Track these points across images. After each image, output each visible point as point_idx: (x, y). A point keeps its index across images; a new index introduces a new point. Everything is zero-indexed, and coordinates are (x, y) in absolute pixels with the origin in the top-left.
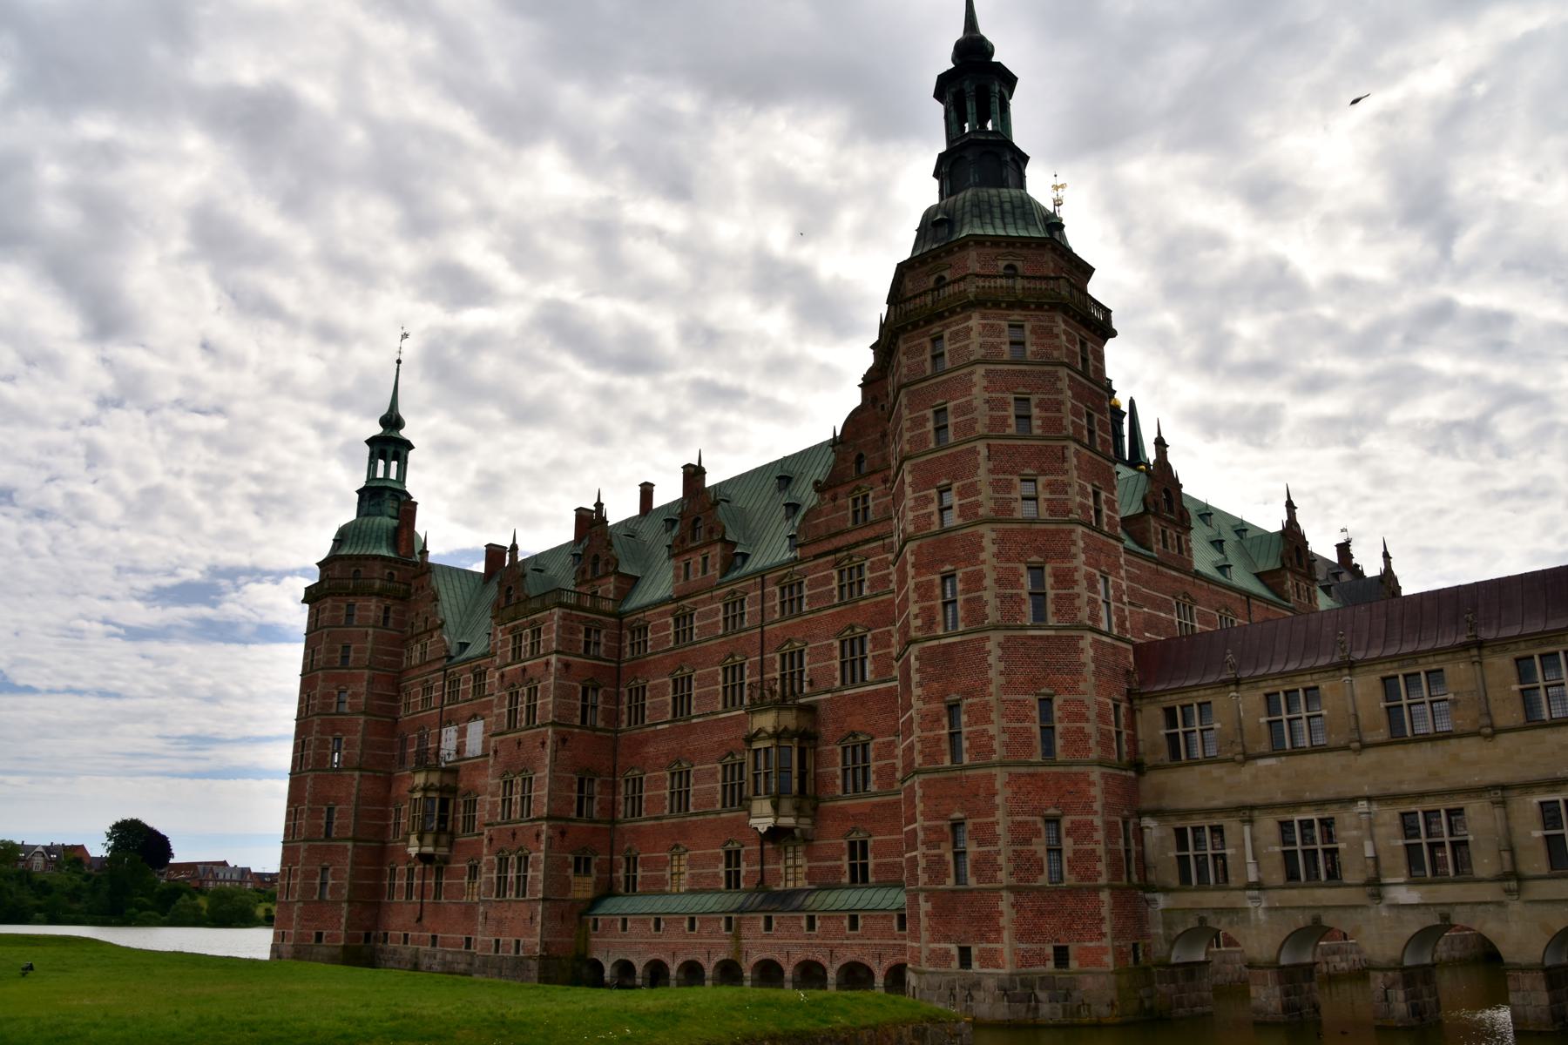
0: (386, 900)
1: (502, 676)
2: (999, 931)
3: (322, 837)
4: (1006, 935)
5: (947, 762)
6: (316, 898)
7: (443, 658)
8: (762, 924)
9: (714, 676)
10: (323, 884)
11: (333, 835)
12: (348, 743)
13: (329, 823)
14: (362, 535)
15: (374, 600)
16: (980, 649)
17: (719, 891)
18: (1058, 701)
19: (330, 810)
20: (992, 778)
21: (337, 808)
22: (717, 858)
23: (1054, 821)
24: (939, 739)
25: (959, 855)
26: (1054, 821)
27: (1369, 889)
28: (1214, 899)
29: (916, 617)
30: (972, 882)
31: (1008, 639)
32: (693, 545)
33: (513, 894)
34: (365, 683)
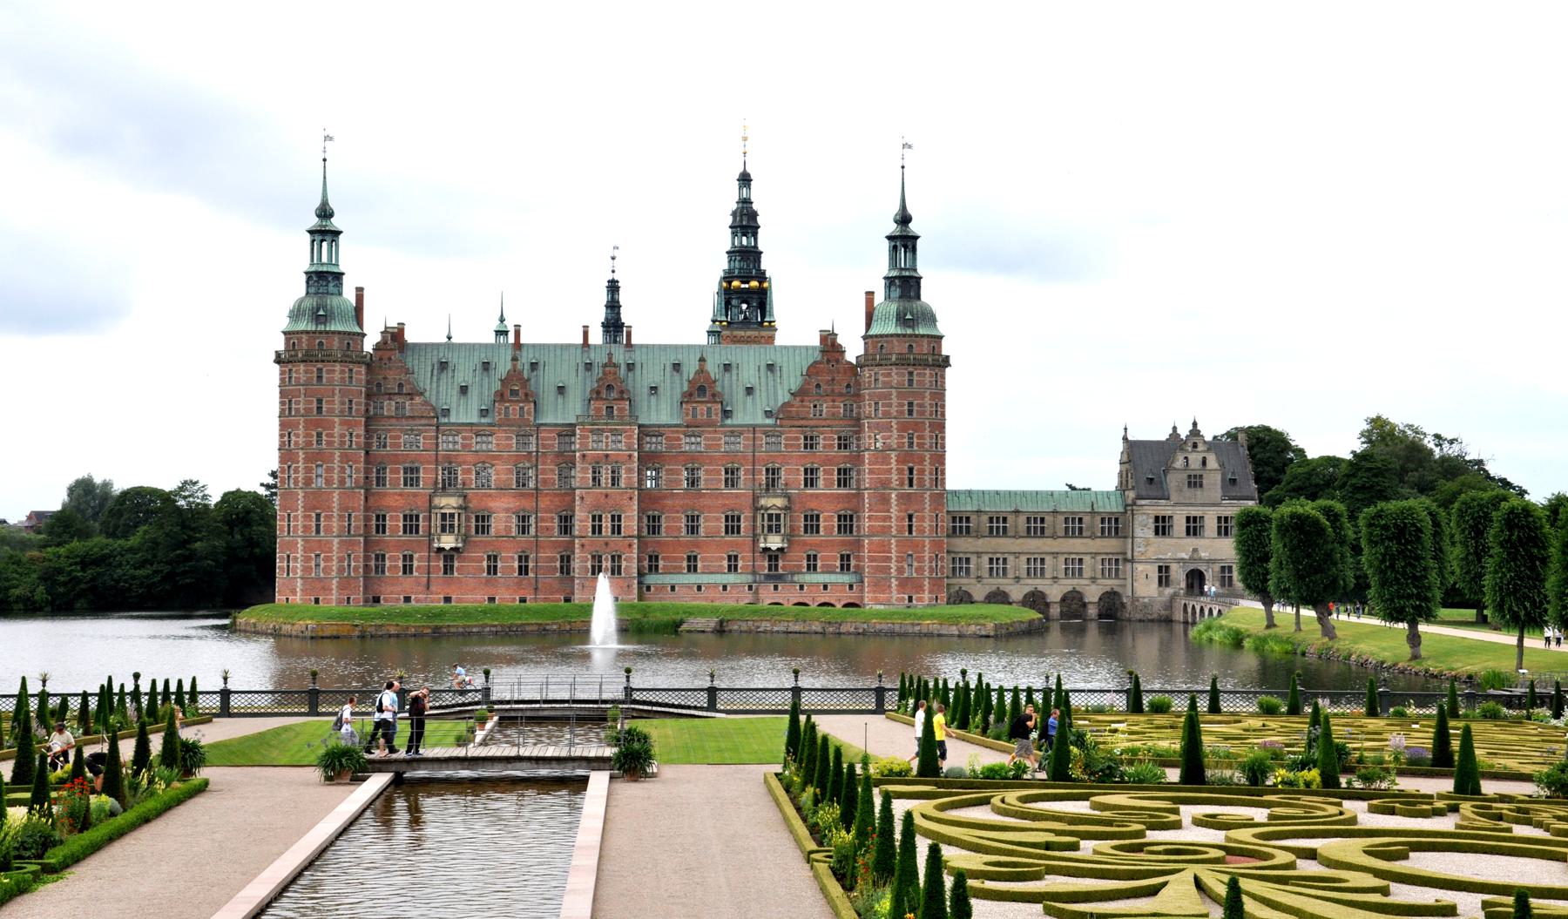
0: (373, 574)
1: (584, 456)
2: (924, 591)
4: (926, 592)
5: (907, 534)
6: (346, 574)
8: (772, 588)
9: (718, 472)
10: (349, 566)
11: (352, 532)
13: (349, 525)
16: (922, 496)
19: (350, 515)
20: (924, 542)
21: (353, 515)
22: (723, 559)
23: (937, 556)
24: (904, 526)
26: (937, 556)
28: (964, 581)
30: (915, 575)
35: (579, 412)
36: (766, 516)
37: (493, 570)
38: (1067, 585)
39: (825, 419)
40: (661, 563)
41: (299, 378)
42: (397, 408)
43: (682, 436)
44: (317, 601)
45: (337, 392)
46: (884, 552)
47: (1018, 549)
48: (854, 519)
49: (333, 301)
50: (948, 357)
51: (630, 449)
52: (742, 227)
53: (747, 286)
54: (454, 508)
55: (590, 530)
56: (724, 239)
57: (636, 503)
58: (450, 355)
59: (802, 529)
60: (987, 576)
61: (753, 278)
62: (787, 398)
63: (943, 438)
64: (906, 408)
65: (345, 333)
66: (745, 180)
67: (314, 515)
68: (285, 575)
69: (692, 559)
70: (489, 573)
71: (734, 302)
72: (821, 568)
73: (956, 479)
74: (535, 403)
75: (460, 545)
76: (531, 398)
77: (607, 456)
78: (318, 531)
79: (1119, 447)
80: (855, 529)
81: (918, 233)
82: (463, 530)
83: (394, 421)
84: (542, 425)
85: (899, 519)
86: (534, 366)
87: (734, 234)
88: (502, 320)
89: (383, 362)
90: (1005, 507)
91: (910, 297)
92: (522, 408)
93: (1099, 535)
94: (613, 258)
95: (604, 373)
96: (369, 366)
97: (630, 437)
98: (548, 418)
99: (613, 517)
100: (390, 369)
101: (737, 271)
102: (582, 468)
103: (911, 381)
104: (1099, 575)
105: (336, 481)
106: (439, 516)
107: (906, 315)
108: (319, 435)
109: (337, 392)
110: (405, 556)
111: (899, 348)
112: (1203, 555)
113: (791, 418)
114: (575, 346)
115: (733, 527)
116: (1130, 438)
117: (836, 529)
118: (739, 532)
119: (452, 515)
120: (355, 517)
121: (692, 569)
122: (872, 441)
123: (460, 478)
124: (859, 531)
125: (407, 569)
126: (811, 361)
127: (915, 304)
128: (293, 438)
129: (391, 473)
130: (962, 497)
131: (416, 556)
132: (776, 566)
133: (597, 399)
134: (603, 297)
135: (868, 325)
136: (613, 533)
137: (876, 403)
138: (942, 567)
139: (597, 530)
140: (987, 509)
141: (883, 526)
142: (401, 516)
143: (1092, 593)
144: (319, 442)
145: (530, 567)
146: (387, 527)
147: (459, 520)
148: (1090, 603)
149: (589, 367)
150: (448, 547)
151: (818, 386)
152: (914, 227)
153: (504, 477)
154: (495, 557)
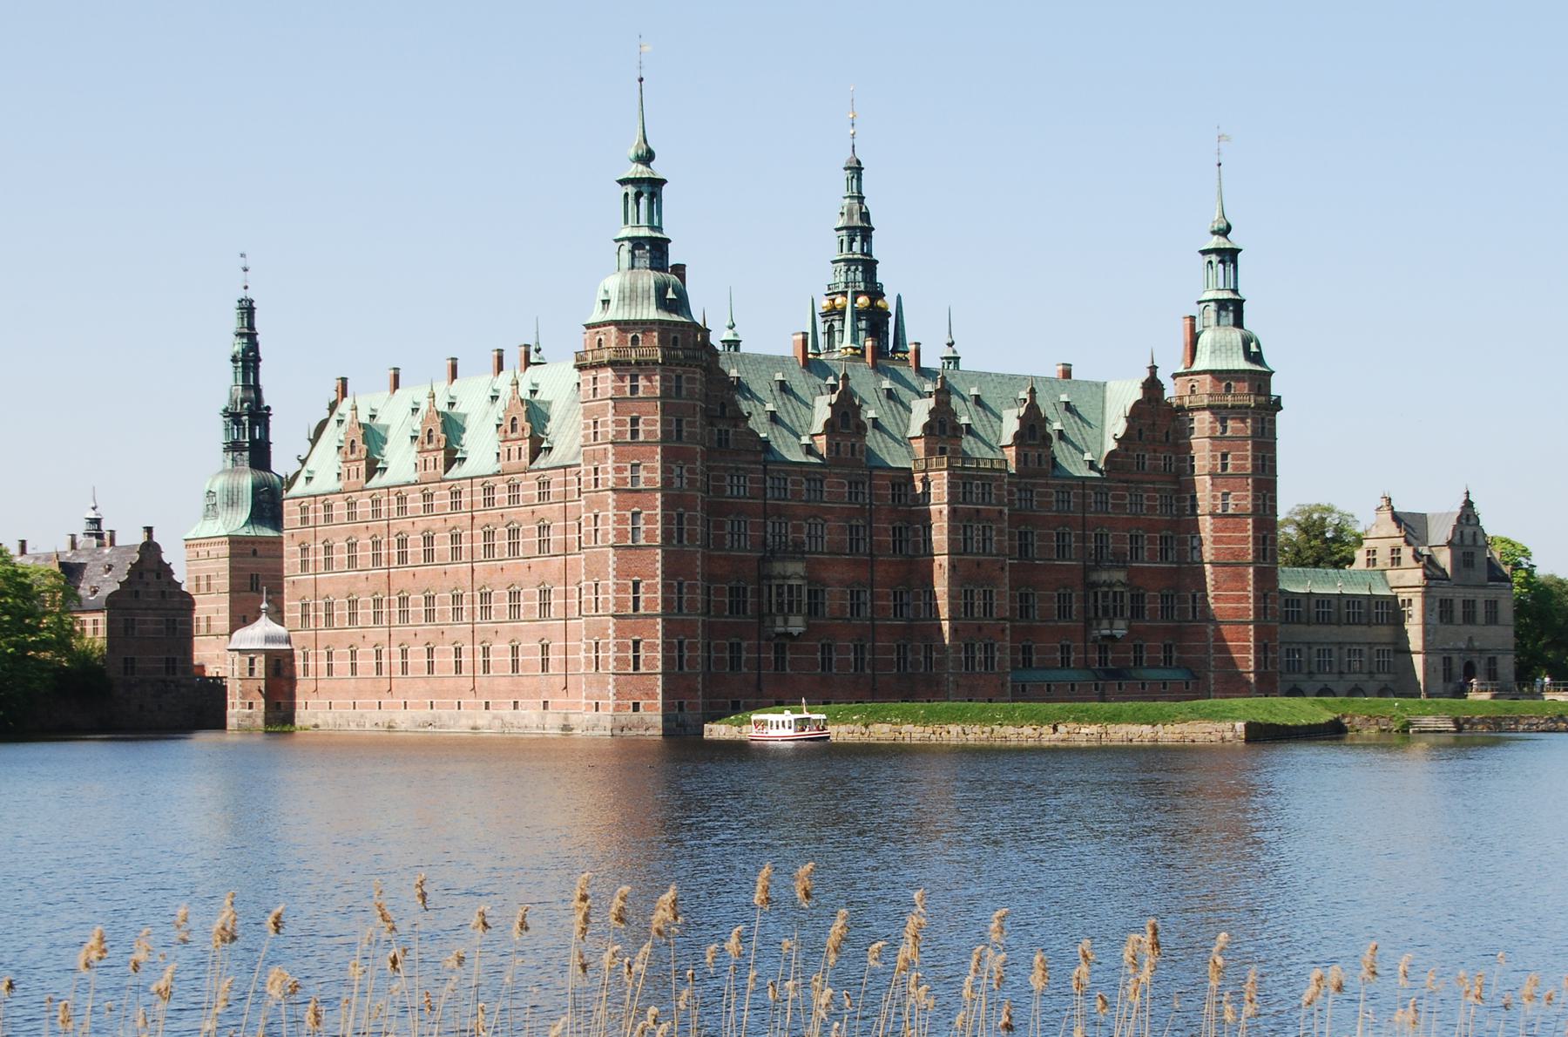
17: (1058, 668)
25: (1266, 658)
32: (1032, 442)
33: (983, 670)
37: (826, 664)
46: (1238, 640)
51: (1000, 503)
56: (831, 246)
57: (1007, 574)
70: (823, 669)
77: (978, 511)
78: (680, 609)
94: (246, 270)
97: (1000, 487)
105: (699, 537)
109: (698, 409)
112: (1476, 644)
128: (643, 474)
131: (744, 644)
134: (233, 322)
141: (1237, 609)
145: (867, 660)
150: (795, 634)
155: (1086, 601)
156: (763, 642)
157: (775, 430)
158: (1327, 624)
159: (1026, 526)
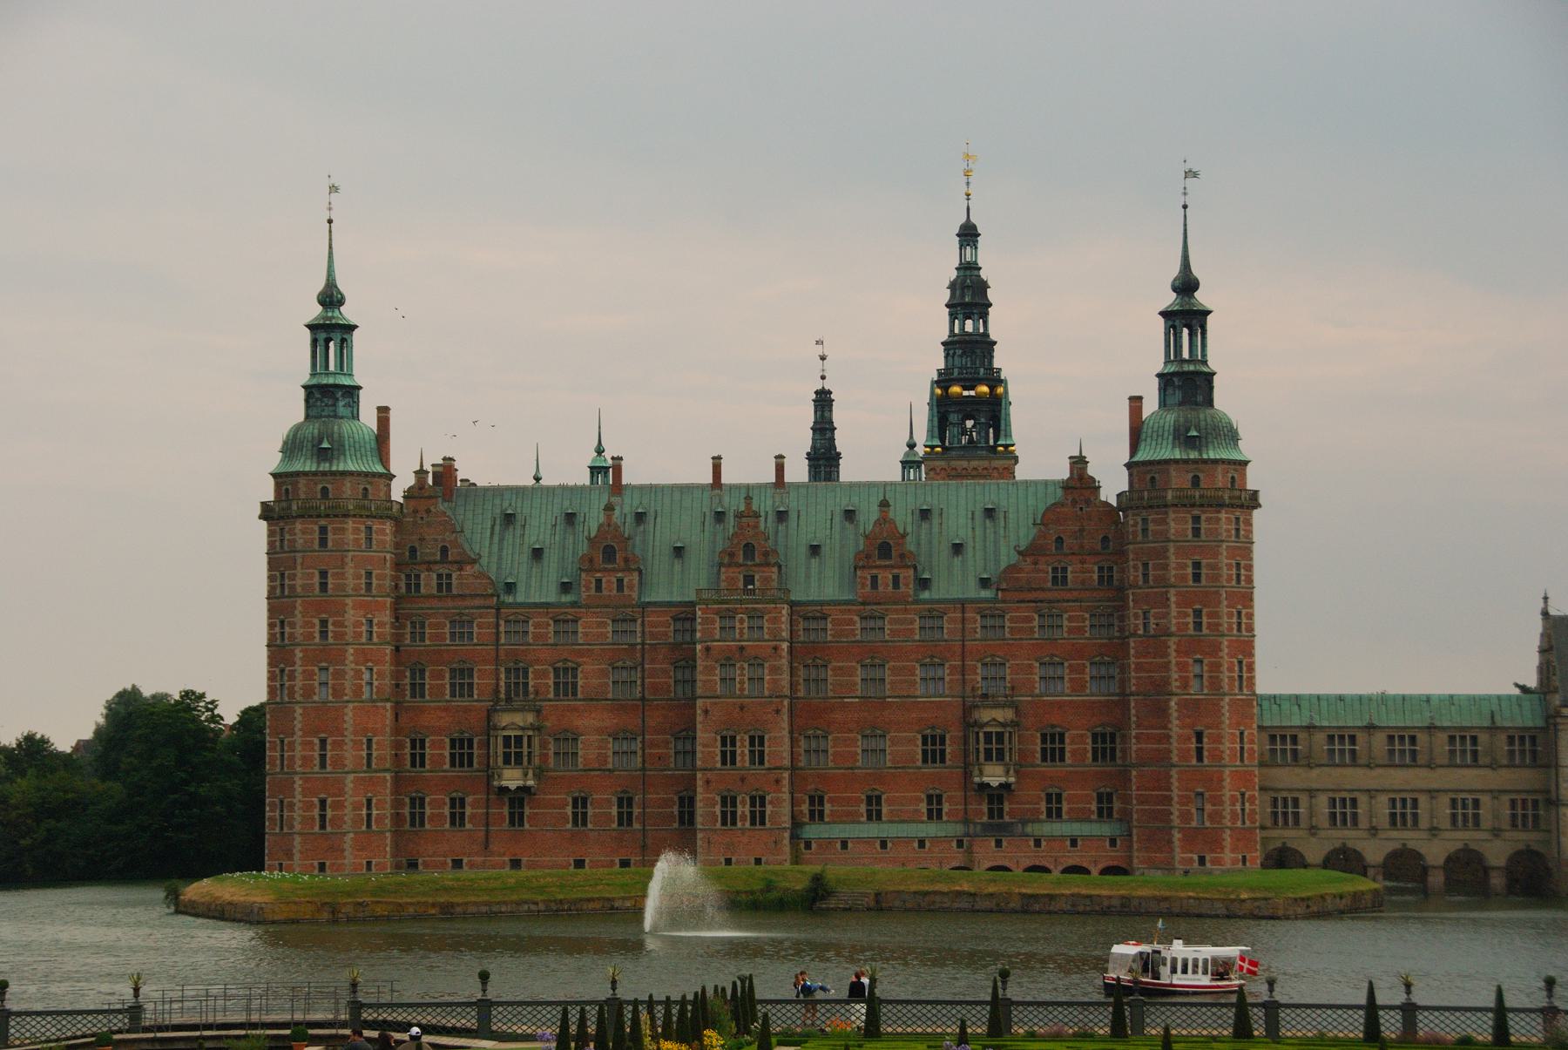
1: (708, 649)
2: (1222, 849)
3: (365, 768)
4: (1227, 851)
5: (1194, 762)
7: (492, 595)
8: (993, 844)
11: (374, 766)
12: (379, 673)
13: (369, 755)
14: (357, 446)
15: (388, 524)
17: (922, 822)
18: (1246, 733)
19: (369, 741)
20: (1222, 773)
21: (375, 740)
23: (1243, 795)
24: (1189, 750)
26: (1243, 795)
27: (1373, 832)
28: (1289, 833)
29: (1176, 680)
30: (1208, 824)
31: (1231, 700)
33: (748, 824)
34: (388, 612)
35: (703, 584)
36: (981, 735)
37: (580, 819)
38: (1452, 841)
39: (1071, 590)
40: (827, 808)
41: (295, 541)
42: (440, 585)
43: (856, 618)
44: (322, 867)
45: (348, 560)
46: (1160, 790)
47: (1373, 785)
48: (1118, 740)
49: (347, 427)
50: (1256, 493)
52: (964, 305)
53: (972, 393)
54: (523, 729)
55: (718, 758)
56: (940, 325)
57: (786, 717)
58: (519, 505)
59: (1038, 756)
60: (1326, 824)
61: (981, 381)
62: (1014, 558)
63: (1250, 616)
64: (1190, 570)
65: (359, 474)
66: (968, 235)
67: (316, 741)
68: (277, 830)
69: (874, 801)
70: (575, 823)
71: (953, 418)
72: (1068, 813)
73: (1271, 678)
74: (640, 572)
75: (531, 783)
76: (633, 564)
77: (742, 648)
78: (323, 765)
79: (1537, 626)
80: (1118, 754)
81: (1209, 306)
82: (536, 761)
83: (435, 603)
84: (649, 603)
85: (1184, 739)
86: (640, 517)
87: (953, 317)
88: (600, 451)
89: (419, 515)
90: (1351, 720)
91: (1197, 404)
92: (620, 581)
93: (1505, 762)
94: (823, 358)
95: (741, 528)
96: (398, 522)
97: (775, 620)
98: (659, 594)
99: (752, 739)
100: (429, 525)
101: (956, 371)
102: (706, 667)
103: (1197, 532)
104: (1506, 825)
106: (500, 740)
107: (1188, 430)
108: (324, 623)
110: (453, 800)
111: (1179, 480)
113: (1020, 590)
114: (702, 487)
115: (934, 752)
116: (1552, 612)
117: (1090, 755)
118: (943, 760)
119: (519, 739)
120: (377, 743)
121: (874, 815)
122: (1140, 622)
123: (531, 683)
124: (1124, 758)
125: (457, 819)
126: (1051, 501)
127: (1203, 414)
128: (287, 629)
129: (432, 677)
130: (1285, 706)
131: (469, 800)
132: (1001, 811)
133: (729, 565)
134: (808, 415)
135: (1134, 447)
136: (752, 762)
137: (1146, 565)
138: (1253, 812)
139: (729, 758)
140: (1325, 723)
142: (447, 740)
143: (1497, 853)
144: (324, 634)
146: (427, 757)
147: (529, 746)
148: (1493, 868)
149: (720, 516)
151: (1059, 540)
152: (1202, 297)
153: (595, 681)
154: (584, 801)
155: (966, 743)
156: (492, 797)
157: (534, 569)
158: (1407, 766)
159: (872, 658)
